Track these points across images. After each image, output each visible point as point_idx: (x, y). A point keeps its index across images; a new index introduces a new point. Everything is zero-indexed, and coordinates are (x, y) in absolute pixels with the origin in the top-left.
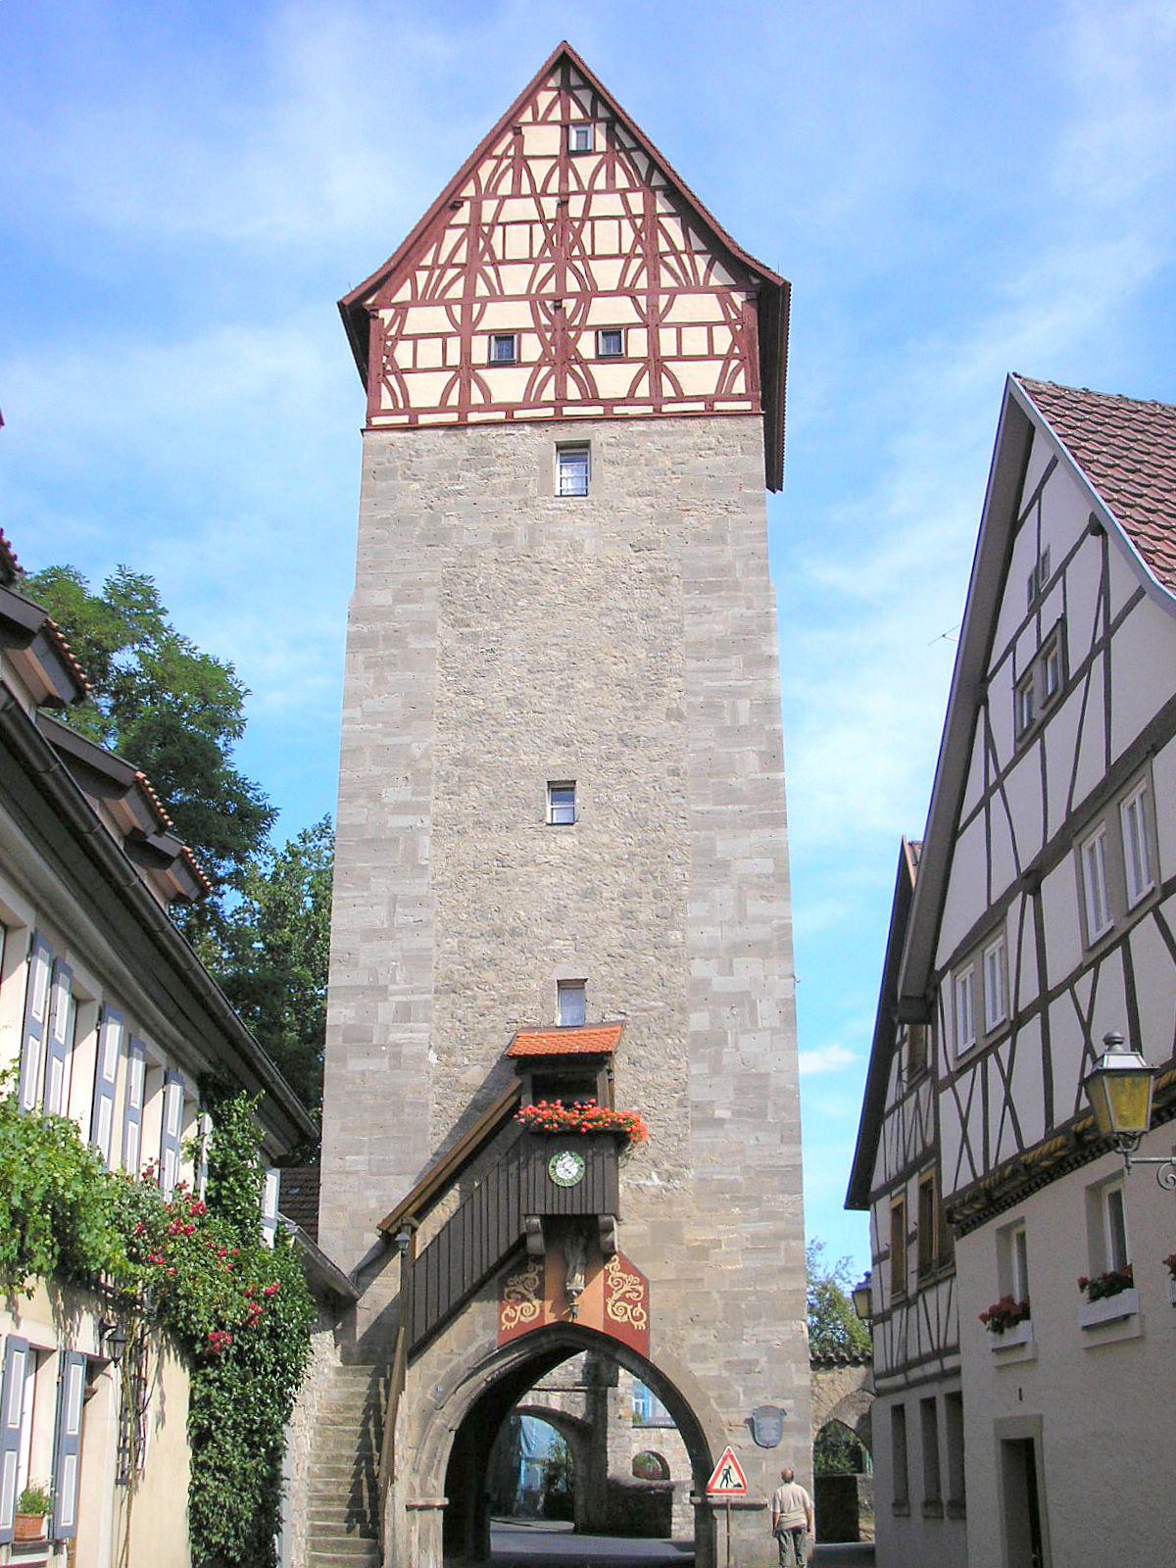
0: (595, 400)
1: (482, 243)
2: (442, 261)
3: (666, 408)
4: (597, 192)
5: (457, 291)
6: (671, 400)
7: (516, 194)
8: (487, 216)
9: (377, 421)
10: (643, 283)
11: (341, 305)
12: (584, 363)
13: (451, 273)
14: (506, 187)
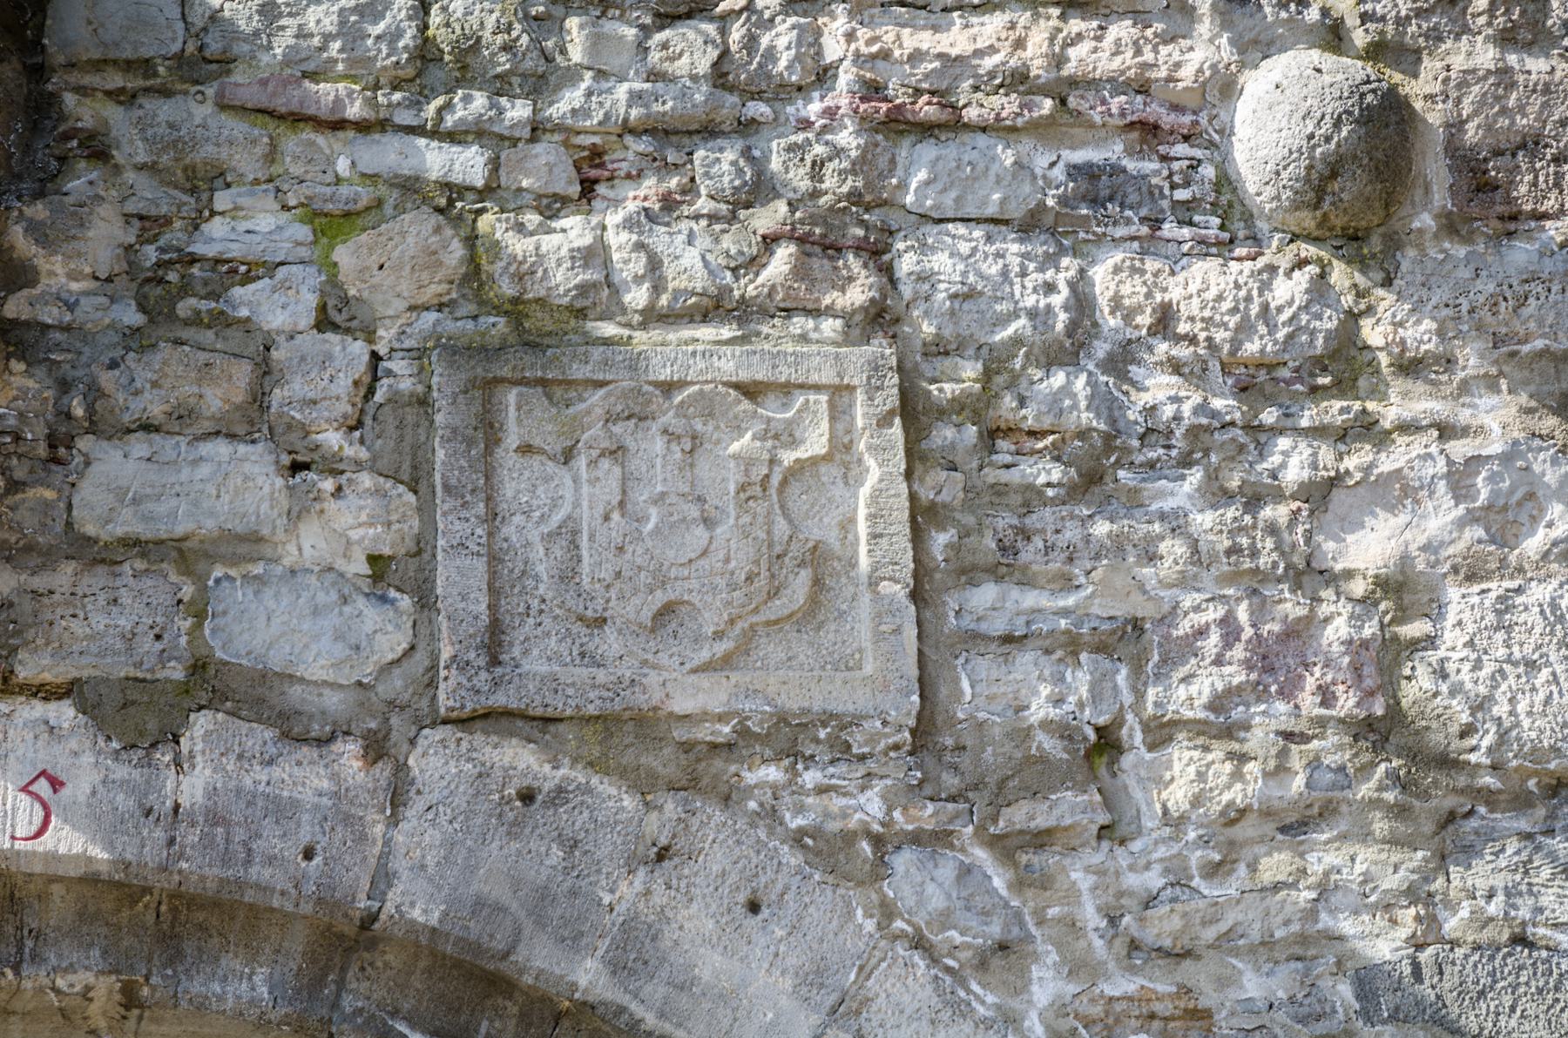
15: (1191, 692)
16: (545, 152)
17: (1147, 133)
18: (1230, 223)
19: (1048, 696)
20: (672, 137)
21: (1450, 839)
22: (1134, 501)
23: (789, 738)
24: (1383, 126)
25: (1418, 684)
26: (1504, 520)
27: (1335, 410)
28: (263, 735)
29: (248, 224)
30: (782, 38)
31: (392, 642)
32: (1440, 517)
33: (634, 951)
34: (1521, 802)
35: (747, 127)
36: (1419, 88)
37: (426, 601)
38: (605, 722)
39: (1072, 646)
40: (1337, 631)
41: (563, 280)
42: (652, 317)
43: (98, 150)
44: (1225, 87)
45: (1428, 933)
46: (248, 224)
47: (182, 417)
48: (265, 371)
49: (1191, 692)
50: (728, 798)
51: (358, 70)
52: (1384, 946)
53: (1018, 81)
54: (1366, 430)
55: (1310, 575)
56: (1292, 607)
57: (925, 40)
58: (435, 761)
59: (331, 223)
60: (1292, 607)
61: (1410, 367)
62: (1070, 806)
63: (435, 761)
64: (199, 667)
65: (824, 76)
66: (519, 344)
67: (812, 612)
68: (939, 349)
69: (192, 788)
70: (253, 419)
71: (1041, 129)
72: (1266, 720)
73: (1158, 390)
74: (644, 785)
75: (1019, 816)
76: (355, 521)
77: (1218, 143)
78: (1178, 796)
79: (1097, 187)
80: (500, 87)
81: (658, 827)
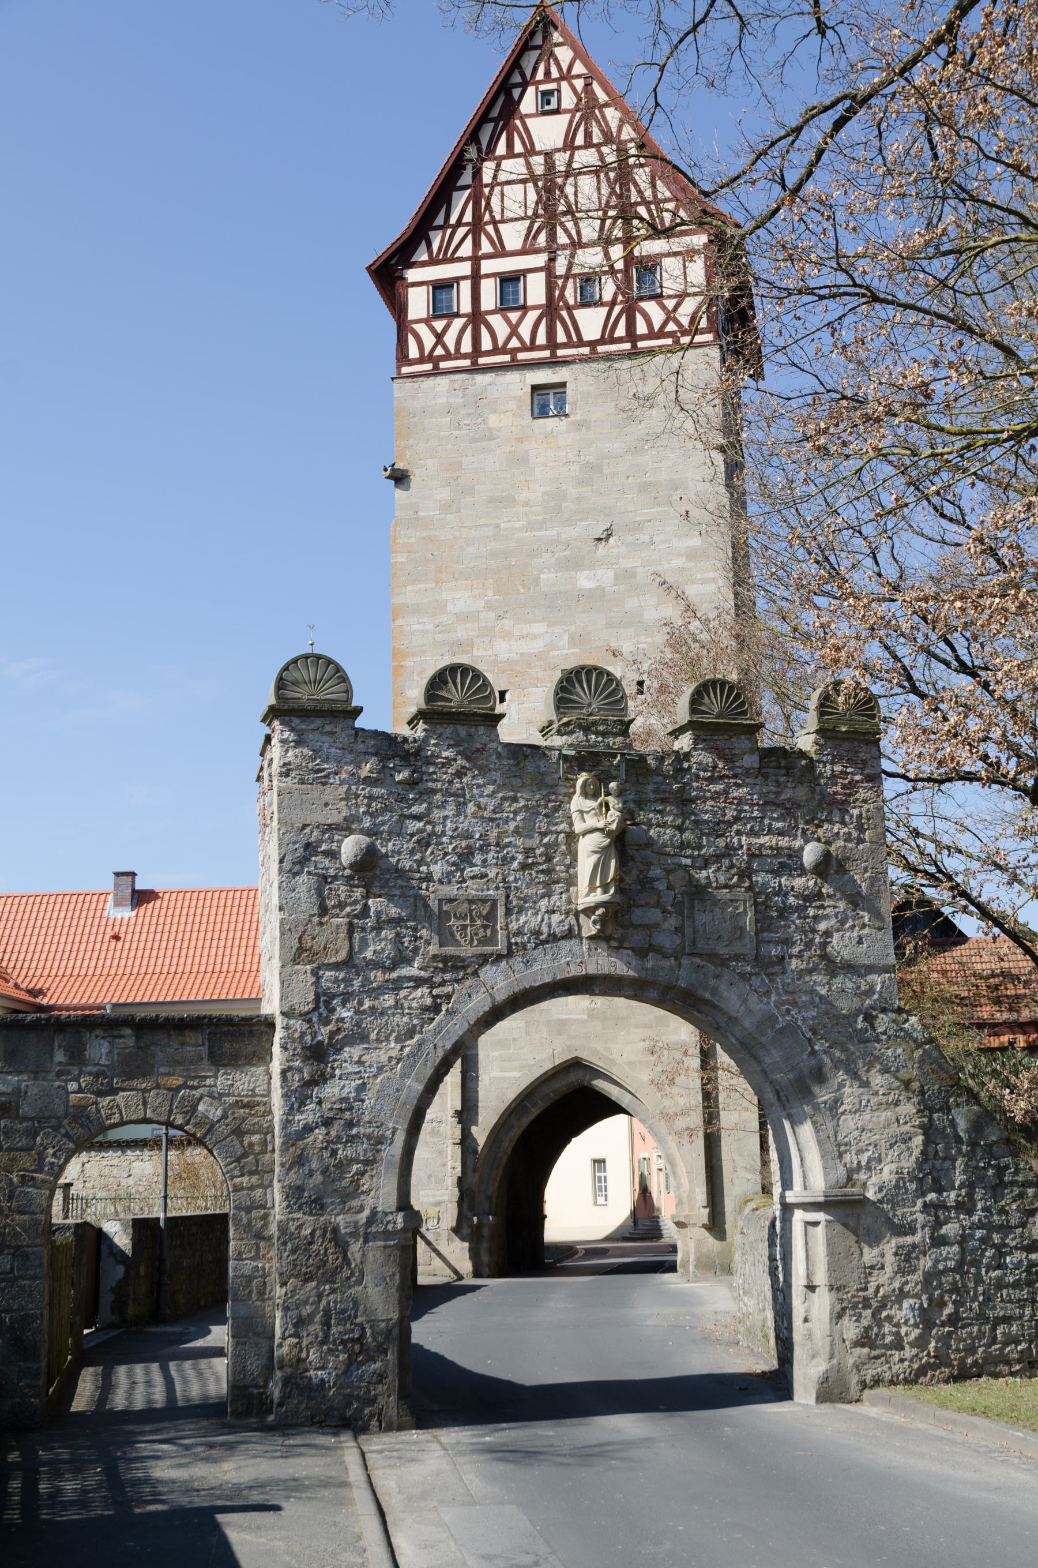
0: (581, 343)
1: (483, 203)
2: (453, 220)
3: (641, 344)
4: (580, 148)
5: (466, 250)
6: (643, 338)
7: (511, 154)
8: (487, 178)
9: (405, 370)
10: (617, 233)
11: (368, 269)
12: (569, 309)
13: (461, 231)
14: (501, 149)
15: (795, 950)
16: (700, 860)
17: (790, 856)
18: (802, 871)
19: (775, 951)
20: (718, 857)
21: (833, 975)
22: (786, 919)
23: (737, 958)
24: (827, 855)
25: (829, 949)
26: (843, 922)
27: (818, 903)
28: (659, 957)
29: (656, 872)
30: (735, 840)
31: (678, 941)
32: (833, 921)
33: (714, 991)
34: (843, 968)
35: (730, 855)
36: (832, 849)
37: (683, 934)
38: (710, 955)
39: (777, 943)
40: (817, 940)
41: (703, 882)
42: (717, 888)
43: (633, 859)
44: (802, 849)
45: (830, 989)
46: (656, 872)
47: (647, 904)
48: (659, 897)
49: (795, 950)
50: (728, 967)
51: (672, 846)
52: (823, 992)
53: (771, 848)
54: (822, 907)
55: (814, 931)
56: (810, 936)
57: (757, 841)
58: (685, 961)
59: (669, 872)
60: (810, 936)
61: (829, 896)
62: (777, 969)
63: (685, 961)
64: (651, 945)
65: (741, 847)
66: (698, 892)
67: (740, 938)
68: (759, 893)
69: (650, 965)
70: (658, 905)
71: (775, 856)
72: (807, 954)
73: (791, 900)
74: (715, 964)
75: (771, 970)
76: (672, 922)
77: (801, 858)
78: (793, 967)
79: (782, 865)
80: (693, 849)
81: (718, 972)
